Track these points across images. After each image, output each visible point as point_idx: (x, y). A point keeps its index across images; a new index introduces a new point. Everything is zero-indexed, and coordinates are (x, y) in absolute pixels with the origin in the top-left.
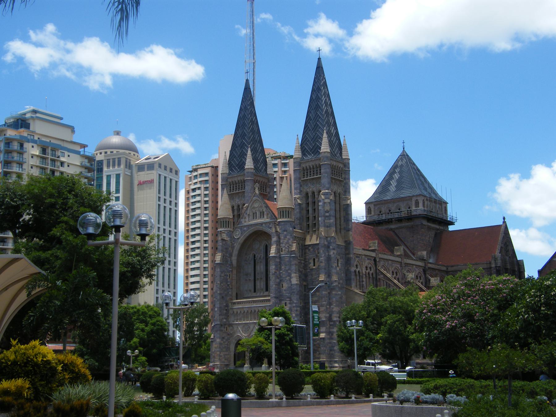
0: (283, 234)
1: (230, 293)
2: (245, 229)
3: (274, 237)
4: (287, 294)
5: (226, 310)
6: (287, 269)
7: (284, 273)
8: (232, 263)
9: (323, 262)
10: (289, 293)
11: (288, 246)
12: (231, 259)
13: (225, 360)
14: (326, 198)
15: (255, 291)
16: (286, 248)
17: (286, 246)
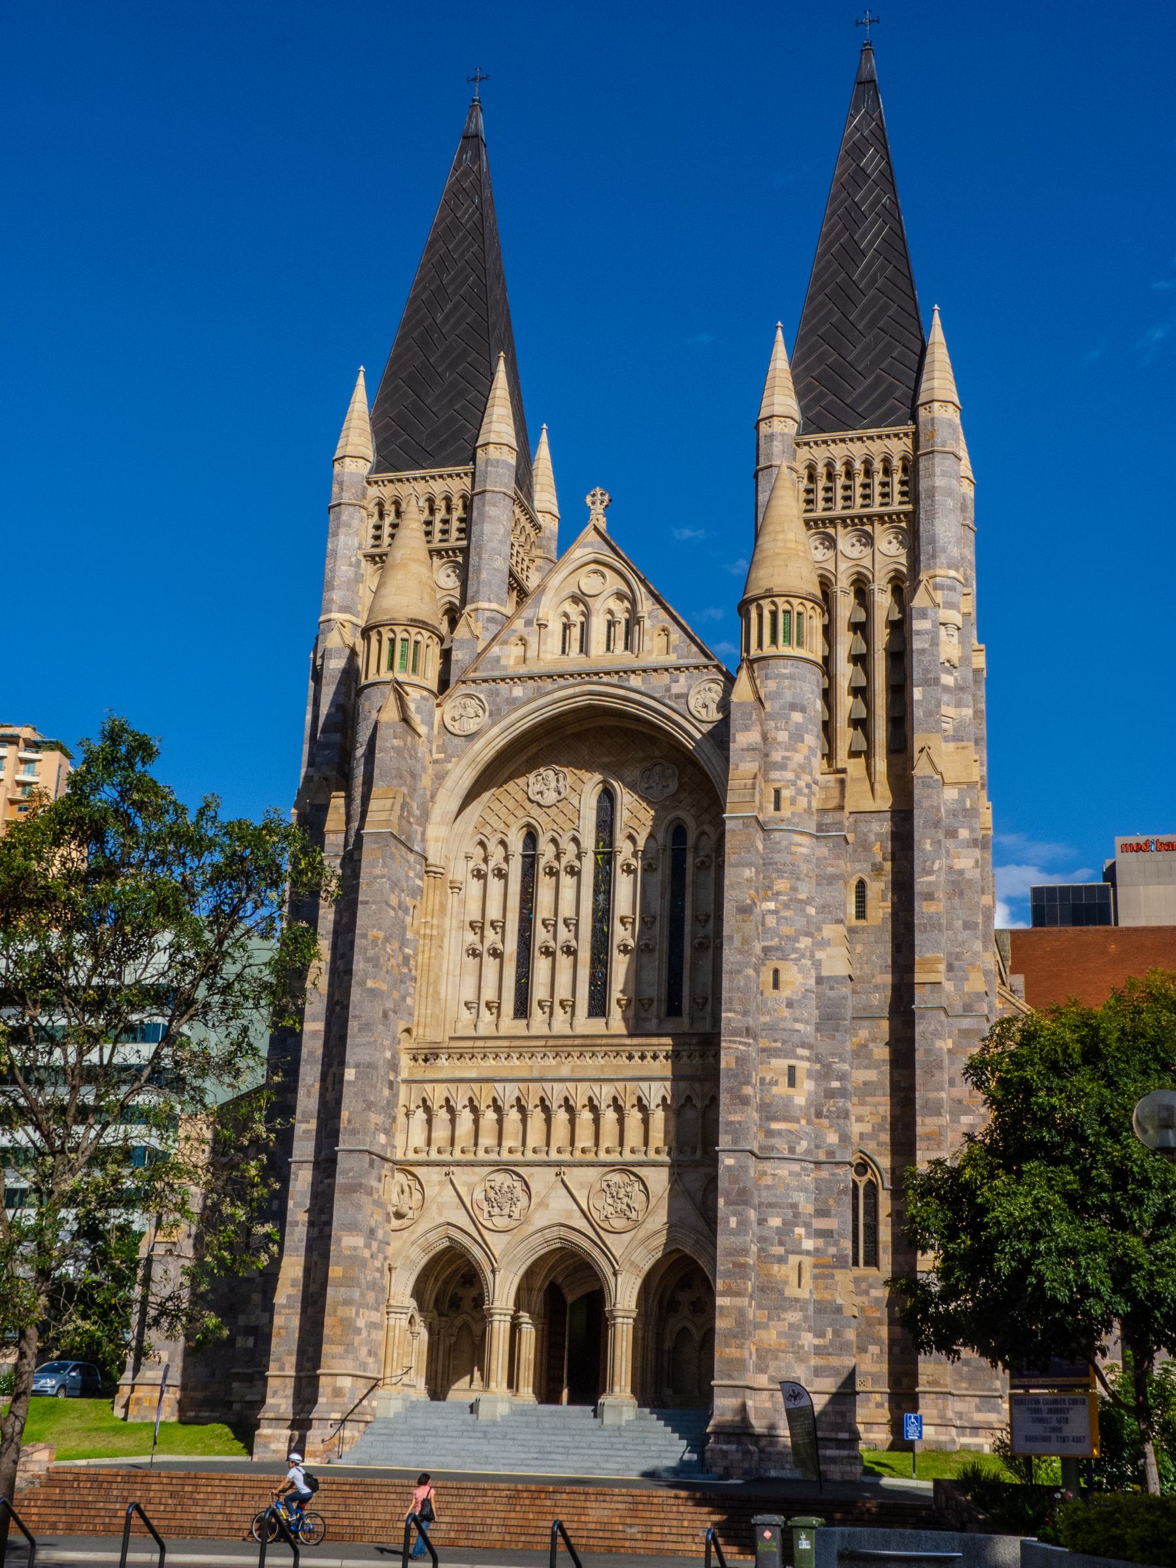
0: (787, 719)
1: (409, 1001)
2: (518, 691)
3: (747, 728)
4: (799, 1026)
5: (391, 1085)
6: (802, 896)
7: (787, 914)
8: (424, 851)
9: (940, 894)
10: (807, 1022)
11: (808, 786)
12: (423, 833)
13: (370, 1353)
14: (950, 605)
15: (522, 1010)
16: (799, 792)
17: (801, 784)
